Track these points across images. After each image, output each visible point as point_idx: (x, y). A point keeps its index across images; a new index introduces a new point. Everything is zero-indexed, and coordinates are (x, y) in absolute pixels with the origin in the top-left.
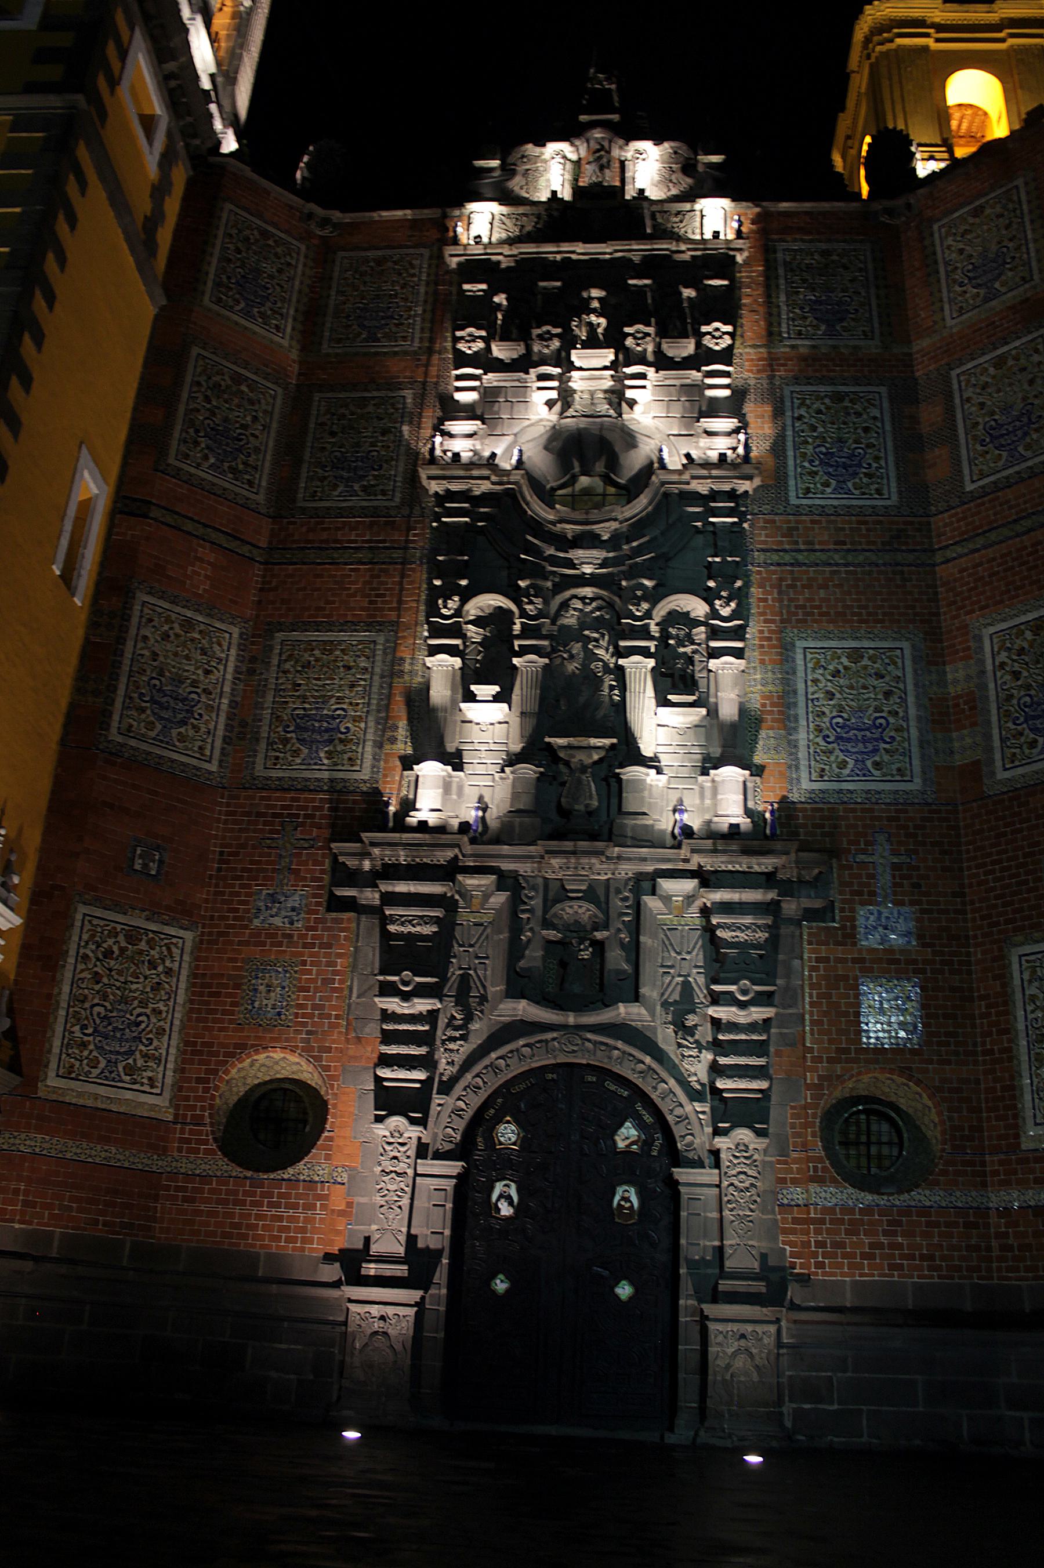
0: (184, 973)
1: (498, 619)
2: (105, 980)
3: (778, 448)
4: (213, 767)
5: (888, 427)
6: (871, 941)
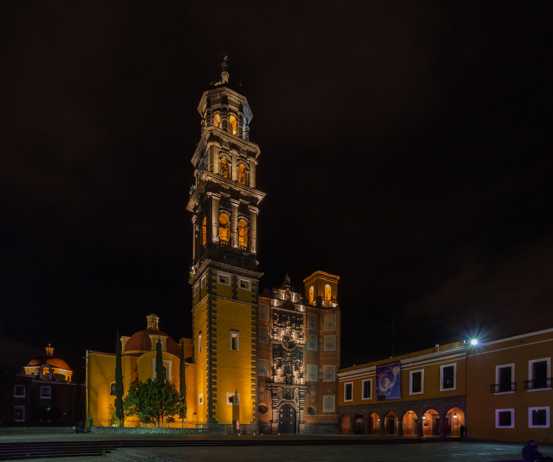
1: (280, 360)
3: (306, 342)
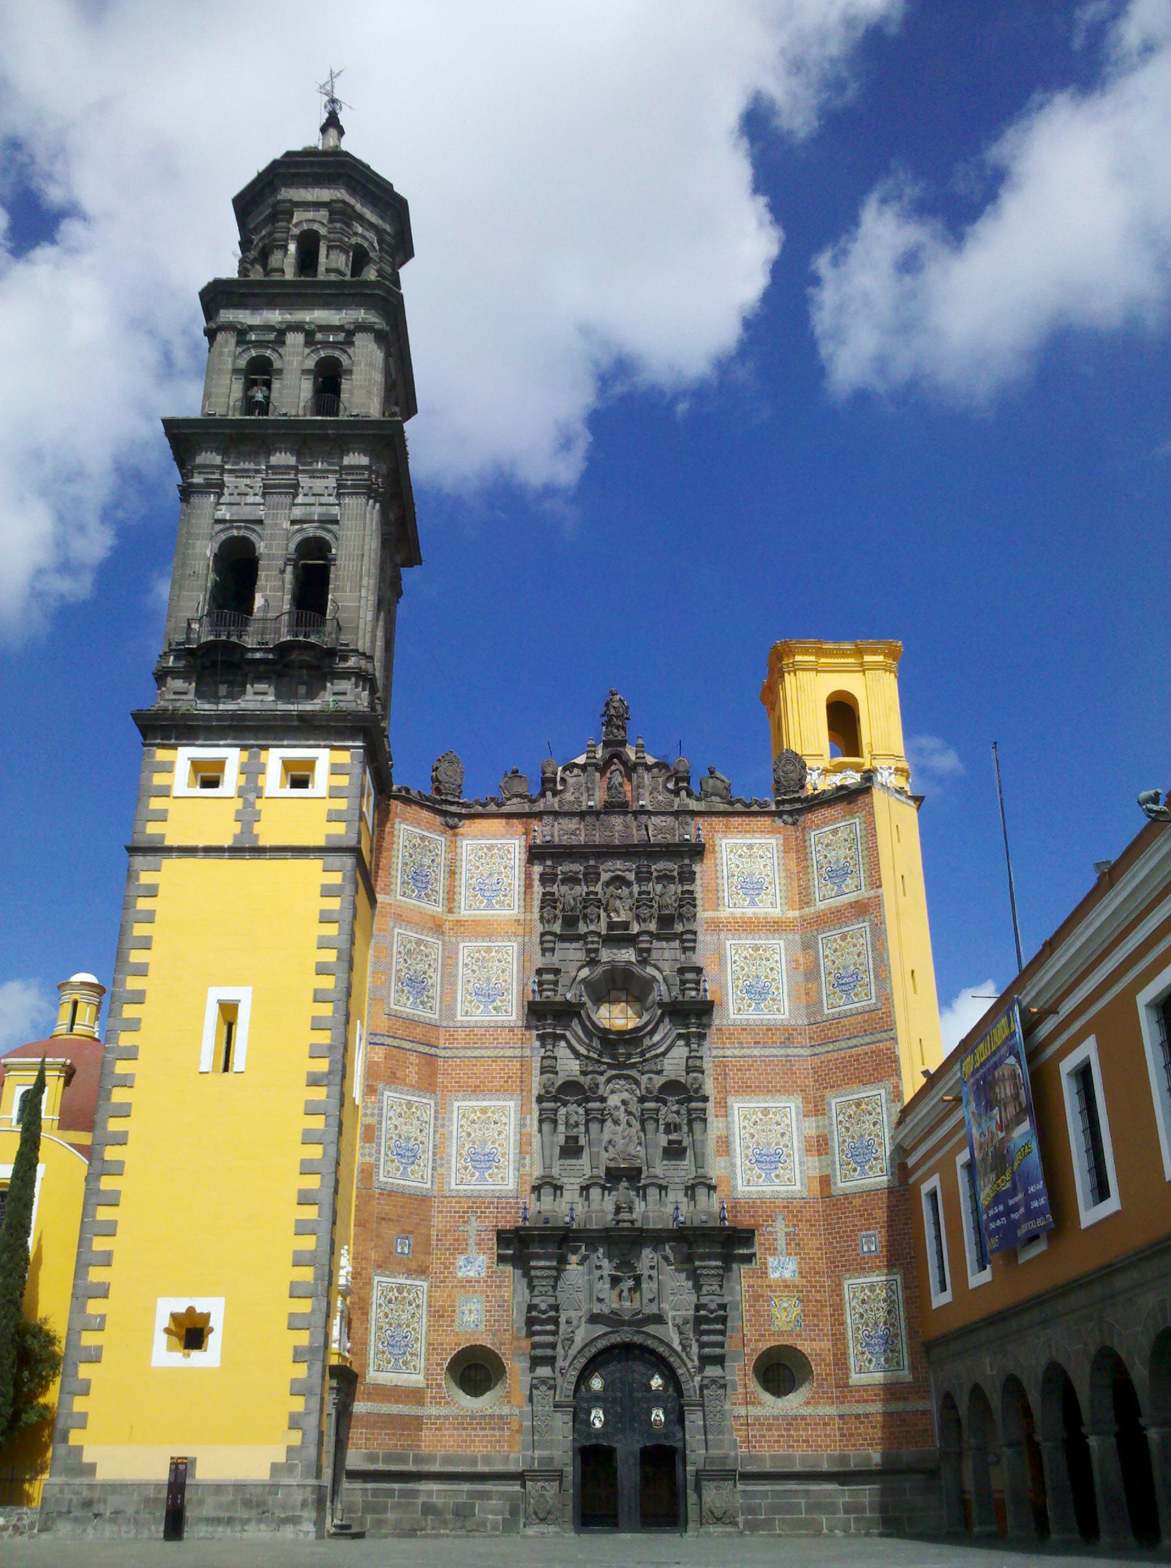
0: (425, 1304)
4: (428, 1186)
5: (784, 967)
6: (774, 1275)
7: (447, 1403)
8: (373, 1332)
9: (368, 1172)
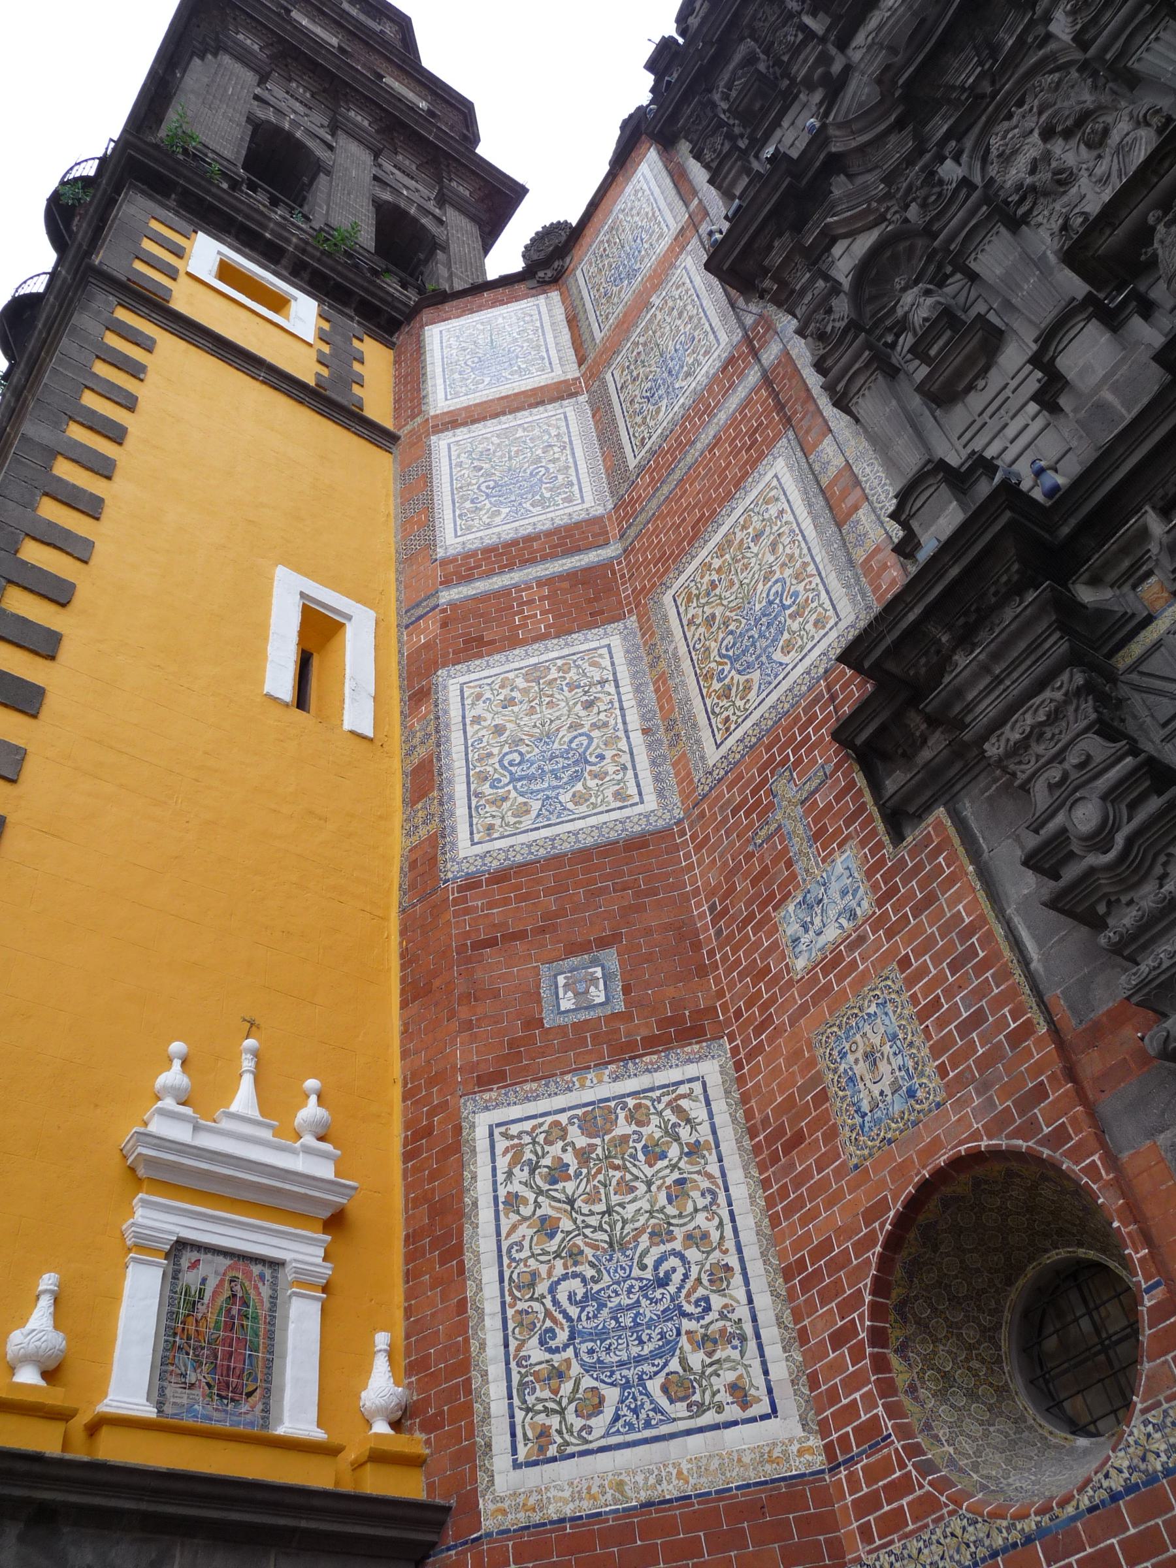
2: (566, 1224)
7: (926, 1506)
8: (491, 1306)
9: (424, 862)
